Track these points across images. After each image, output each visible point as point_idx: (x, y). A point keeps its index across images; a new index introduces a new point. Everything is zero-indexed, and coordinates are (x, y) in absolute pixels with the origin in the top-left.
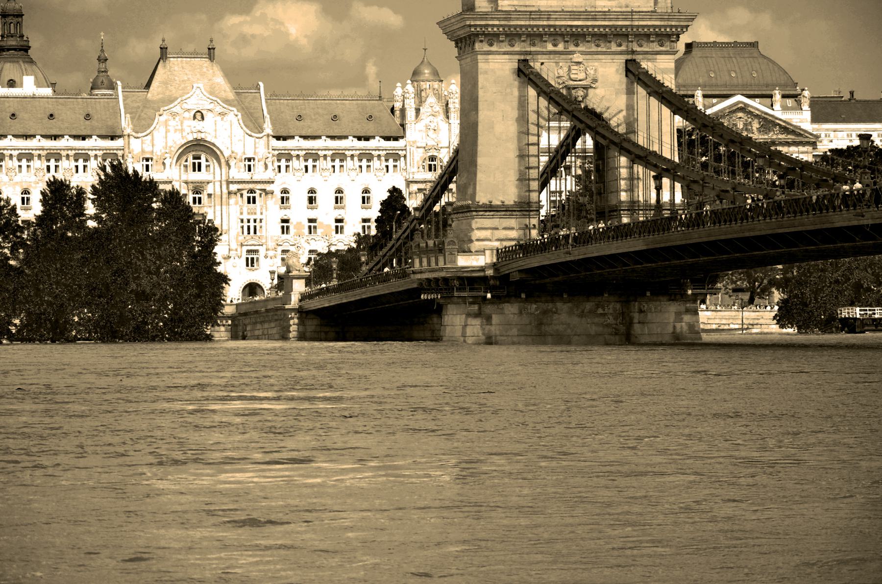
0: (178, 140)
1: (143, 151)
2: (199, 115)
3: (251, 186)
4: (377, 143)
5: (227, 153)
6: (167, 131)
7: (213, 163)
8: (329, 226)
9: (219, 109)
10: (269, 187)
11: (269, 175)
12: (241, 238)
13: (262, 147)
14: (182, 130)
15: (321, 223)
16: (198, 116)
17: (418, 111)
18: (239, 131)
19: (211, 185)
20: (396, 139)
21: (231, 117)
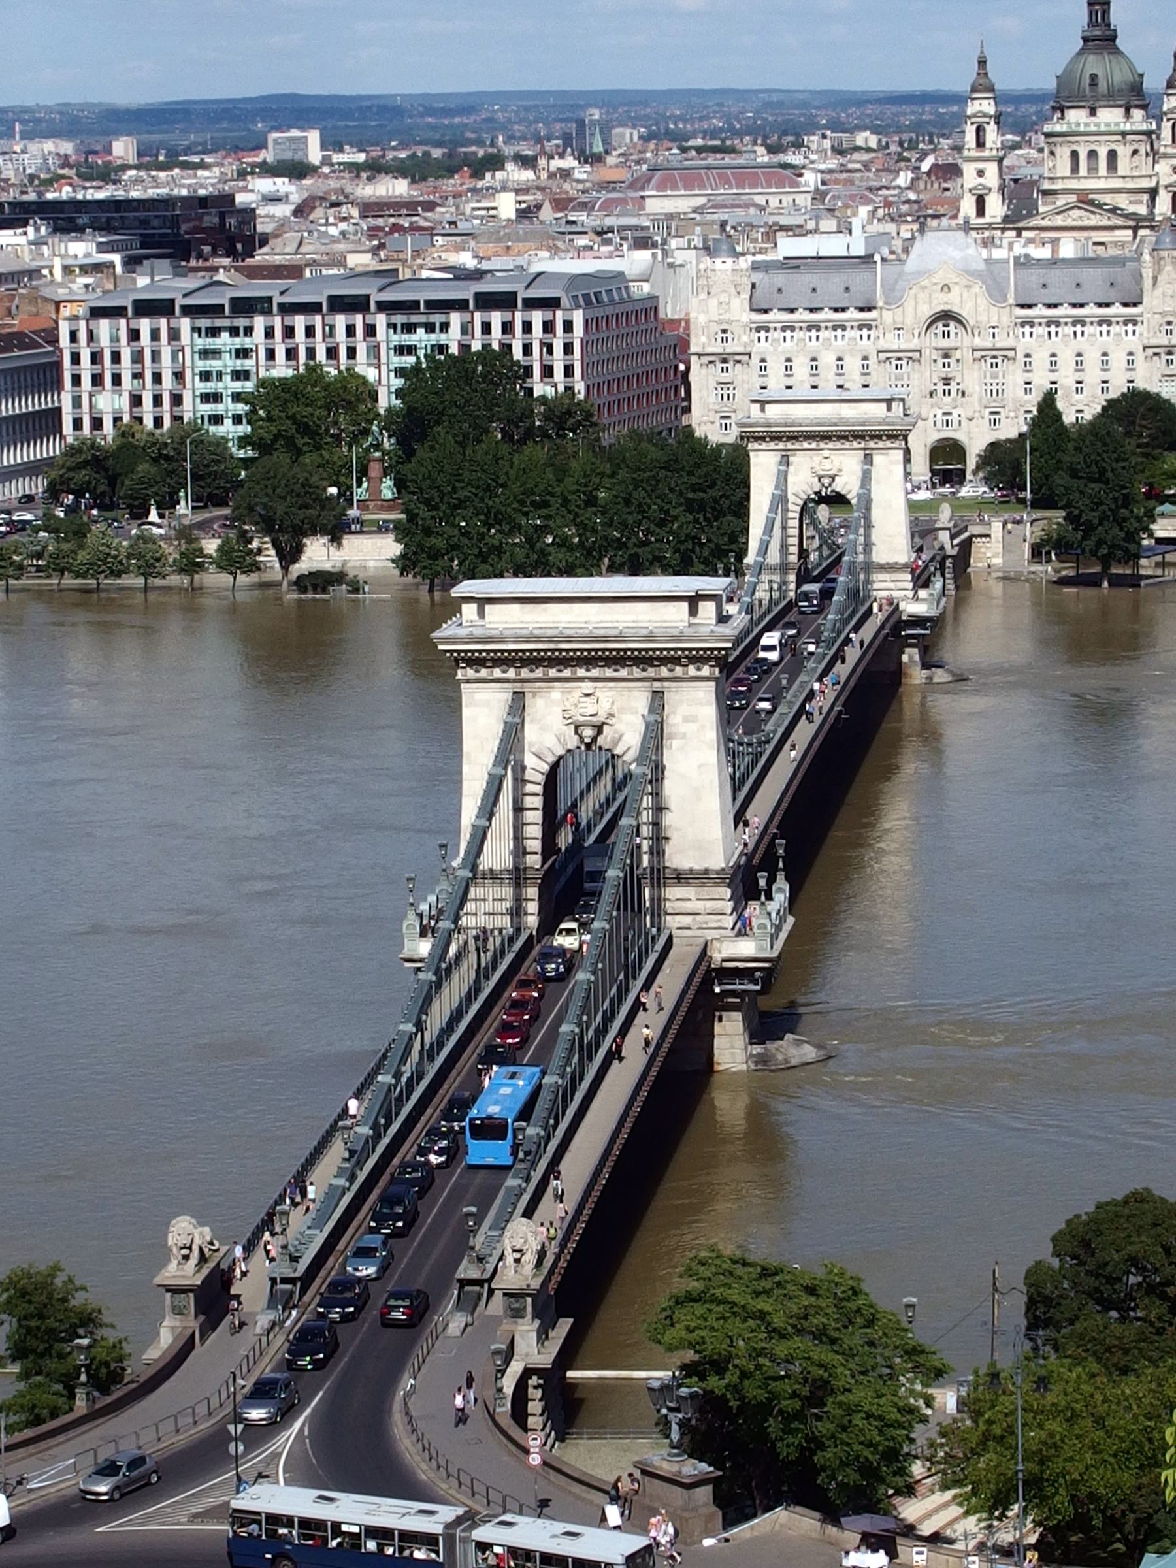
0: (927, 311)
1: (894, 322)
2: (946, 288)
3: (994, 353)
4: (1117, 309)
5: (972, 322)
6: (916, 303)
7: (960, 329)
8: (1070, 388)
9: (964, 282)
10: (1011, 354)
11: (1010, 343)
12: (984, 402)
13: (1006, 316)
14: (930, 302)
15: (1063, 387)
16: (946, 289)
17: (1155, 279)
18: (983, 302)
19: (959, 351)
20: (1135, 305)
21: (976, 289)
